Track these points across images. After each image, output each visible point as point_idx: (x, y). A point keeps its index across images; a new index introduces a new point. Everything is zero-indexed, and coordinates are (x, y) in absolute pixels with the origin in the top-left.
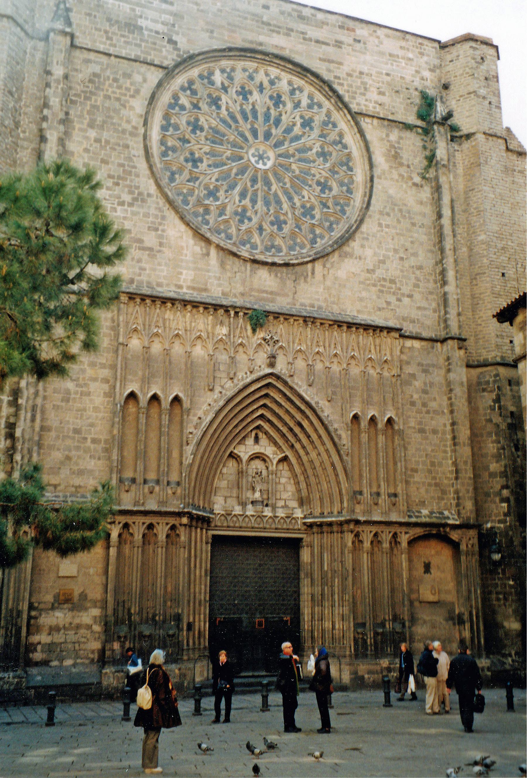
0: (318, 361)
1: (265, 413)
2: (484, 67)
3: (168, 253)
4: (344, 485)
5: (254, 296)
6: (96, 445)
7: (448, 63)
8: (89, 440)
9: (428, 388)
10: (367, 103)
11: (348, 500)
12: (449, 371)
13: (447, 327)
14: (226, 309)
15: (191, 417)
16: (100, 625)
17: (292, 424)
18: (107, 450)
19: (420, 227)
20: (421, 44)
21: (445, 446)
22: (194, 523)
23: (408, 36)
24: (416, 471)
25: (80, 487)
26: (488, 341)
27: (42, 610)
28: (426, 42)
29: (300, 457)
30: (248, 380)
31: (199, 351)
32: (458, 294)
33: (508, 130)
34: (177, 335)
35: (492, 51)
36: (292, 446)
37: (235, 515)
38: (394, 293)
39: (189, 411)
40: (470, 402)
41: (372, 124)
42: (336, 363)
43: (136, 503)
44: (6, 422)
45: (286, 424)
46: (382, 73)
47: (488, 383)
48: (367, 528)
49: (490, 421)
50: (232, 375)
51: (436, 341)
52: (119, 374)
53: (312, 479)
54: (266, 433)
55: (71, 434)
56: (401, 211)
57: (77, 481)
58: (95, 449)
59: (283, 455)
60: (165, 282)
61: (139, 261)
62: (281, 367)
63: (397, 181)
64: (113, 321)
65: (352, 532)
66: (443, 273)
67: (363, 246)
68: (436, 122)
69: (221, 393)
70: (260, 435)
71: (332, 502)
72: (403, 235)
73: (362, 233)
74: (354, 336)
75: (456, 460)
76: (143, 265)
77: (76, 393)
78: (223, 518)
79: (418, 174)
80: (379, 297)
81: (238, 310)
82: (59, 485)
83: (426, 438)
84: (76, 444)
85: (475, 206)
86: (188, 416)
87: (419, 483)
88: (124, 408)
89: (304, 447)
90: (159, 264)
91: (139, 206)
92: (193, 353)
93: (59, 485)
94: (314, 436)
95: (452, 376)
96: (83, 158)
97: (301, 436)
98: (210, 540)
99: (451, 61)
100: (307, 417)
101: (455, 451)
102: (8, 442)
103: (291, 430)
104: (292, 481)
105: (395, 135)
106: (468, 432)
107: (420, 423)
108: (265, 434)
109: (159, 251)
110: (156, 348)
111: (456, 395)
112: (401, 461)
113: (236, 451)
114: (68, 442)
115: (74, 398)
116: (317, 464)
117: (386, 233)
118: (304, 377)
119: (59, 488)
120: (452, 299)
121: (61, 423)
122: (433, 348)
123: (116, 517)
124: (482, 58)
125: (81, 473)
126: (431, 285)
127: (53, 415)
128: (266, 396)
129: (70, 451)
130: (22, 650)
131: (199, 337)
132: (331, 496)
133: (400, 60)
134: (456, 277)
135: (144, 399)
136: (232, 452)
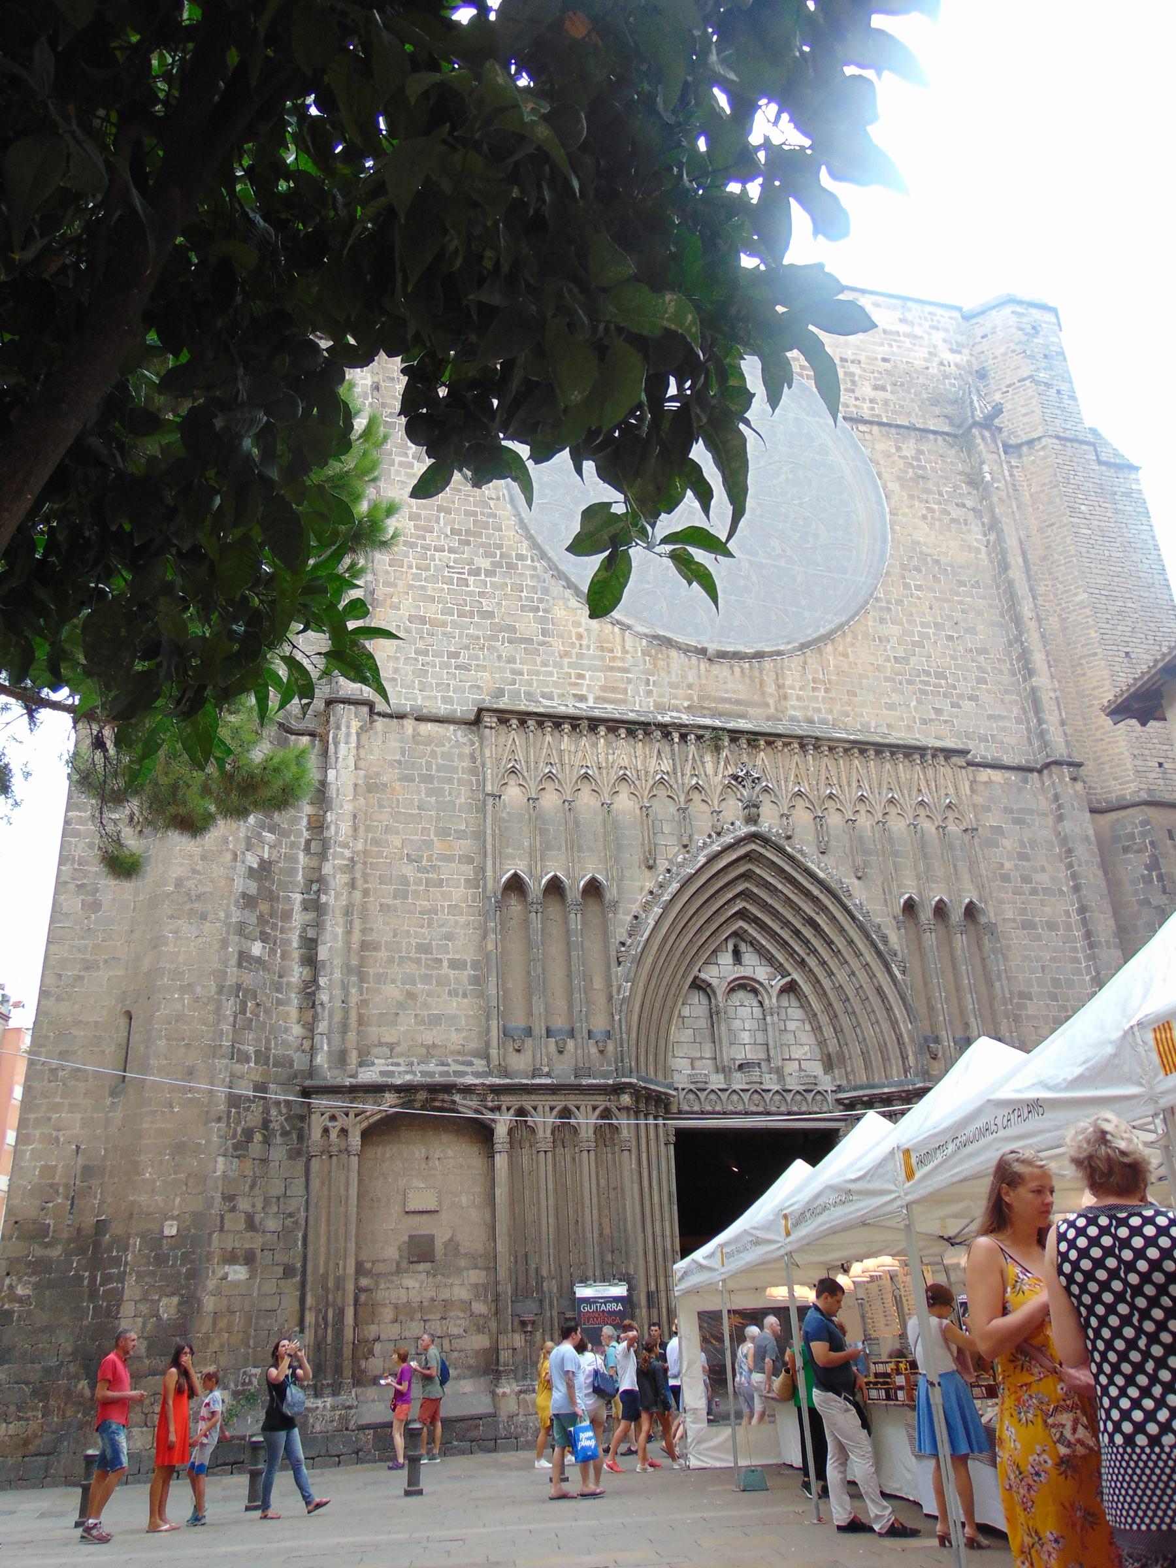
0: (832, 811)
1: (748, 907)
2: (1039, 340)
3: (558, 645)
4: (905, 1027)
5: (708, 709)
7: (978, 339)
8: (445, 964)
10: (858, 403)
11: (915, 1054)
12: (1060, 818)
13: (1045, 744)
14: (666, 730)
15: (620, 916)
16: (485, 1301)
18: (476, 980)
19: (973, 587)
20: (930, 313)
21: (1074, 950)
23: (910, 304)
25: (434, 1046)
26: (1118, 766)
27: (379, 1275)
28: (939, 311)
29: (818, 981)
30: (716, 848)
31: (624, 802)
32: (1055, 691)
33: (1093, 431)
34: (586, 777)
35: (1050, 317)
36: (802, 963)
37: (713, 1091)
38: (945, 696)
39: (615, 905)
40: (1106, 873)
41: (870, 433)
42: (863, 812)
43: (536, 1073)
44: (300, 936)
45: (786, 924)
46: (876, 359)
47: (1132, 836)
49: (1146, 902)
50: (685, 841)
51: (1030, 770)
52: (489, 847)
53: (845, 1020)
54: (752, 943)
56: (937, 562)
57: (429, 1037)
58: (456, 979)
59: (788, 979)
60: (556, 691)
61: (511, 660)
62: (769, 823)
63: (924, 517)
64: (473, 759)
66: (1025, 656)
67: (882, 620)
68: (975, 424)
69: (669, 871)
70: (743, 947)
71: (885, 1059)
72: (949, 601)
73: (877, 599)
74: (888, 766)
75: (1098, 973)
76: (518, 666)
77: (418, 882)
78: (691, 1096)
79: (957, 505)
80: (919, 701)
81: (683, 731)
82: (398, 1044)
83: (1039, 938)
84: (423, 971)
85: (1060, 549)
88: (500, 906)
89: (823, 963)
90: (545, 664)
91: (504, 575)
92: (614, 806)
93: (398, 1044)
94: (840, 943)
95: (1067, 825)
96: (411, 507)
97: (816, 943)
98: (672, 1139)
99: (983, 337)
100: (824, 909)
101: (1092, 957)
102: (306, 972)
103: (797, 933)
104: (808, 1027)
105: (909, 448)
106: (1111, 922)
107: (1023, 912)
108: (752, 944)
109: (543, 644)
110: (550, 800)
111: (1079, 860)
112: (1000, 979)
113: (703, 976)
114: (409, 968)
116: (850, 991)
117: (919, 598)
118: (811, 838)
119: (398, 1049)
120: (1047, 698)
122: (1026, 781)
123: (502, 1098)
124: (1034, 328)
126: (1006, 679)
127: (380, 920)
128: (746, 876)
129: (414, 983)
130: (347, 1351)
131: (624, 778)
132: (883, 1047)
133: (902, 338)
134: (1048, 662)
135: (536, 886)
136: (696, 978)
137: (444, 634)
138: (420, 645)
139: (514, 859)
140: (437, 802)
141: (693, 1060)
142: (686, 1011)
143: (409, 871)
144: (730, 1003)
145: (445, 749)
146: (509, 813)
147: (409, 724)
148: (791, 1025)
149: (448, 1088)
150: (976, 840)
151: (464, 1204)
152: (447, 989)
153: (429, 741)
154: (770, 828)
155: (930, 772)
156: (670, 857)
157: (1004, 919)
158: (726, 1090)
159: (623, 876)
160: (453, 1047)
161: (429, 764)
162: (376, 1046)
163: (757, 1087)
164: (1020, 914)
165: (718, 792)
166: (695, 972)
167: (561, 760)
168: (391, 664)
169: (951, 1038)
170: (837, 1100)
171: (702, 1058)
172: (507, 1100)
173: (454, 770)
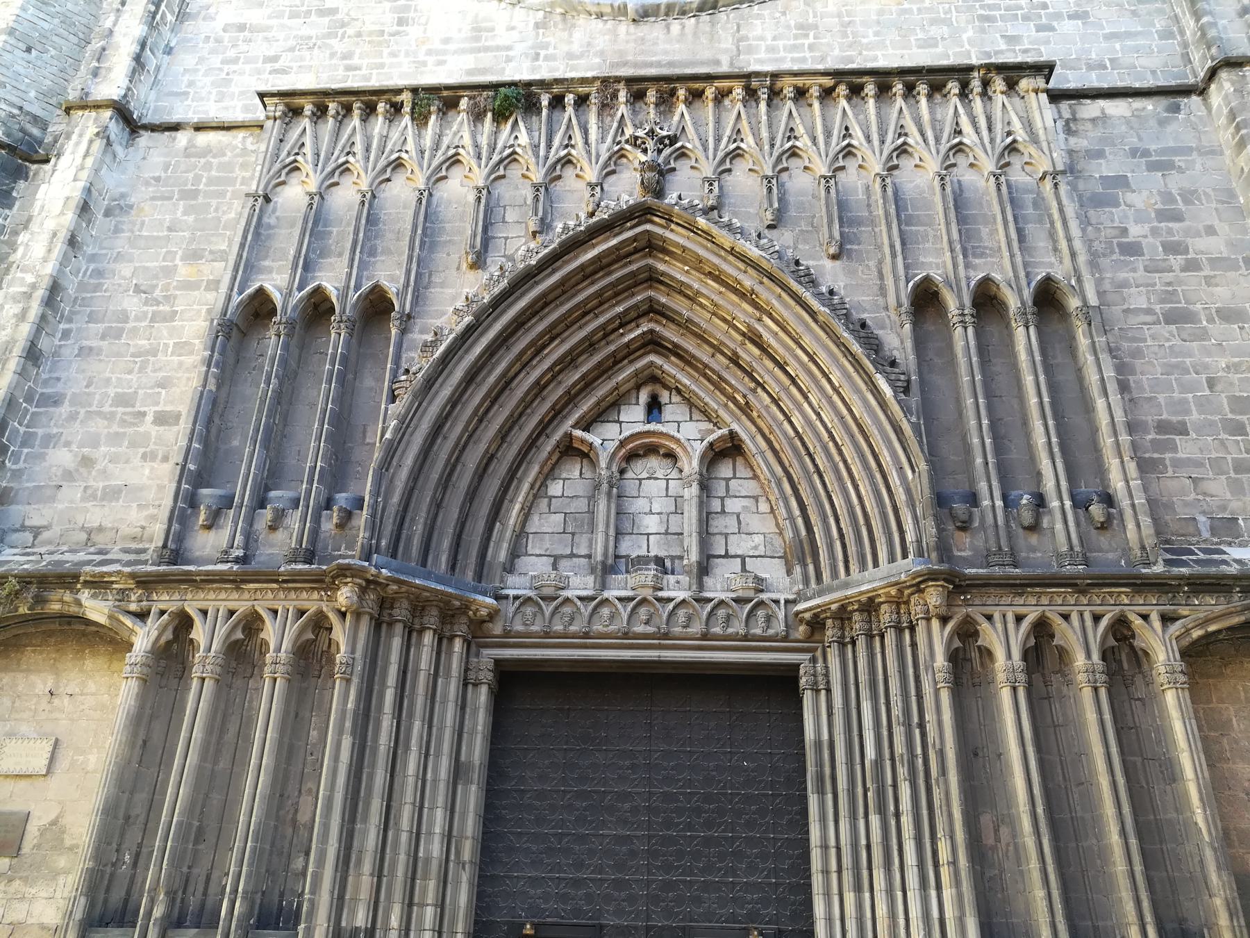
3: (414, 32)
6: (162, 428)
9: (1181, 205)
17: (733, 341)
22: (401, 612)
24: (1182, 430)
25: (100, 529)
37: (567, 600)
38: (1026, 18)
45: (717, 349)
48: (1005, 608)
50: (532, 226)
55: (107, 409)
57: (95, 516)
59: (725, 431)
61: (347, 56)
65: (944, 620)
70: (664, 396)
76: (355, 61)
82: (46, 528)
84: (115, 428)
86: (404, 332)
87: (1199, 464)
90: (393, 55)
93: (46, 528)
97: (765, 370)
98: (487, 676)
103: (735, 360)
104: (764, 507)
107: (1169, 296)
108: (679, 392)
109: (397, 33)
110: (346, 197)
115: (135, 329)
119: (45, 535)
121: (87, 387)
122: (1176, 109)
125: (112, 494)
127: (74, 366)
129: (95, 444)
137: (266, 39)
138: (231, 53)
139: (271, 272)
140: (196, 220)
141: (556, 560)
142: (555, 488)
143: (132, 304)
144: (629, 475)
145: (226, 159)
146: (277, 218)
147: (182, 138)
148: (733, 505)
149: (68, 580)
150: (1063, 188)
151: (91, 767)
152: (142, 450)
153: (207, 151)
154: (680, 197)
155: (978, 104)
156: (509, 252)
157: (1127, 311)
158: (592, 598)
159: (429, 282)
160: (125, 530)
161: (198, 179)
162: (17, 531)
163: (647, 593)
164: (1162, 301)
165: (601, 161)
166: (567, 426)
167: (368, 149)
168: (186, 78)
169: (997, 494)
170: (797, 614)
171: (572, 555)
172: (166, 601)
173: (232, 182)
